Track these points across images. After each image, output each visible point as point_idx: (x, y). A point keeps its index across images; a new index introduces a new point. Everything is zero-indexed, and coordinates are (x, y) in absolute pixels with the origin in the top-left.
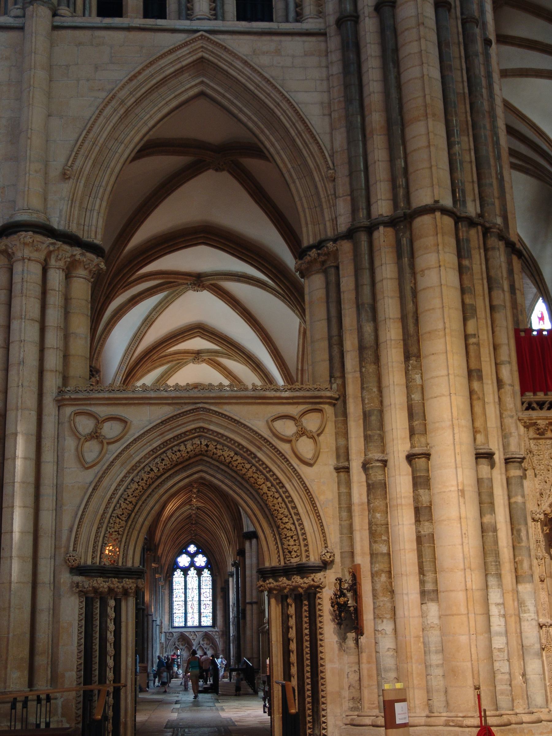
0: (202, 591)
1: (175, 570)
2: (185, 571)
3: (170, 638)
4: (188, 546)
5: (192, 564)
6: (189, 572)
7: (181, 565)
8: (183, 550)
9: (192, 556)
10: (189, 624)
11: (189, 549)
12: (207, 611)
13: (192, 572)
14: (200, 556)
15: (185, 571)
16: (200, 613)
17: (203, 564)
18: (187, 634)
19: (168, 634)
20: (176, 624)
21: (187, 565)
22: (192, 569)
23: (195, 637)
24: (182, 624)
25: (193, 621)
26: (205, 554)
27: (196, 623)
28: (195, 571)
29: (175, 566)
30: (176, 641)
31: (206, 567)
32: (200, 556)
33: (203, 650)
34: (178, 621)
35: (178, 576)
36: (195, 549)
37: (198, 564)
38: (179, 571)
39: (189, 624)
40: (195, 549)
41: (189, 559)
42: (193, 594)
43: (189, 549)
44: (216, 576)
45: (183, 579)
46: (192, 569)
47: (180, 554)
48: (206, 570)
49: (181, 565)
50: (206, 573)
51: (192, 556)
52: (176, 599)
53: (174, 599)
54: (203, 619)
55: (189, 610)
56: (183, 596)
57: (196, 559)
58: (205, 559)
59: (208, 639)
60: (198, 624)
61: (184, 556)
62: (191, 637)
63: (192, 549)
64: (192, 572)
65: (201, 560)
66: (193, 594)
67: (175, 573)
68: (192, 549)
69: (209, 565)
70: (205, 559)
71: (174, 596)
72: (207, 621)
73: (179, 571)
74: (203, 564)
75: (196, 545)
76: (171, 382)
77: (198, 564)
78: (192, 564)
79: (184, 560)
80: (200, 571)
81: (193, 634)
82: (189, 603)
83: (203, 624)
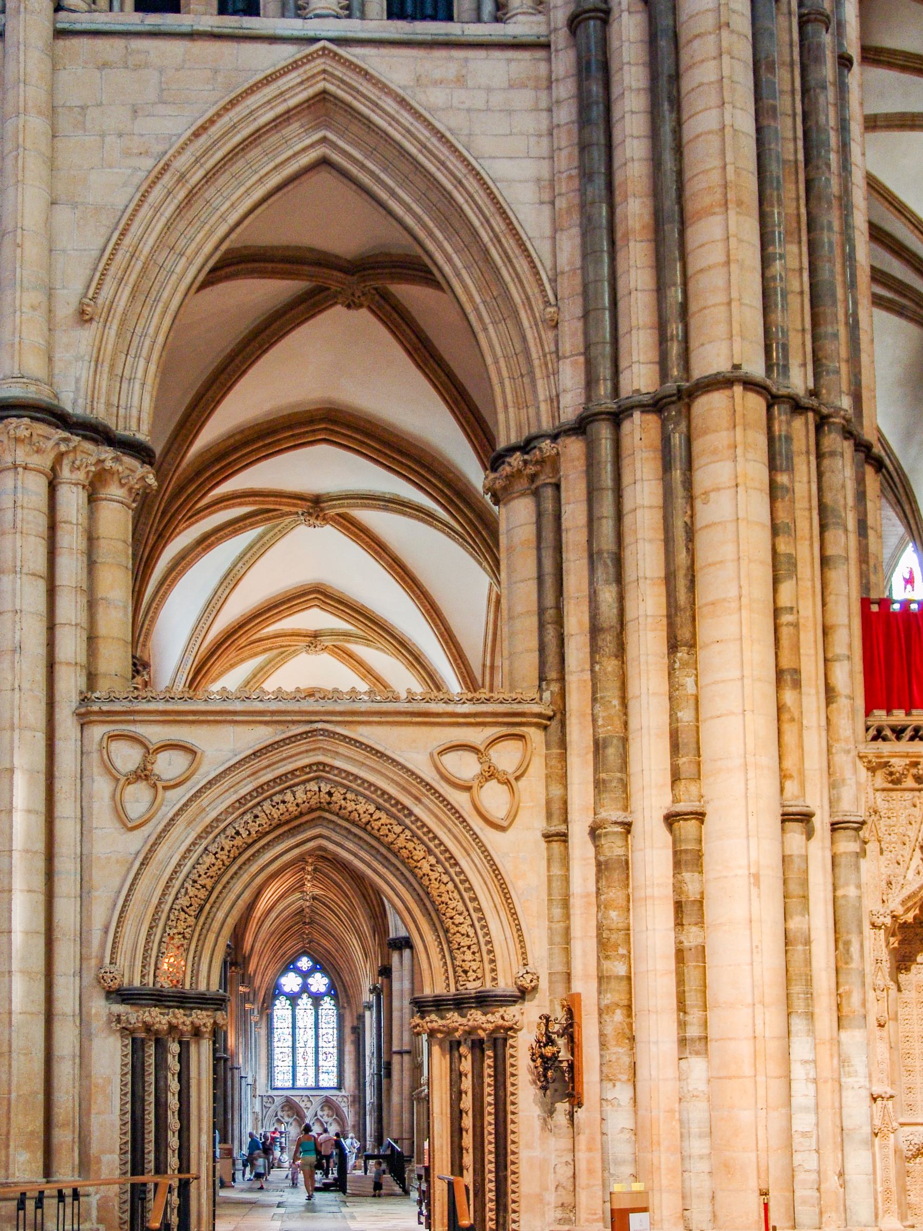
0: (321, 1032)
1: (275, 997)
2: (293, 998)
4: (297, 958)
5: (305, 988)
6: (300, 1001)
8: (289, 966)
9: (305, 975)
10: (300, 1083)
11: (299, 964)
12: (329, 1063)
13: (305, 1002)
14: (318, 975)
15: (293, 998)
16: (317, 1066)
17: (323, 989)
18: (296, 1099)
19: (265, 1099)
20: (278, 1084)
22: (305, 996)
23: (309, 1105)
25: (306, 1078)
26: (325, 972)
27: (311, 1083)
29: (275, 992)
30: (279, 1109)
31: (327, 993)
33: (322, 1124)
34: (282, 1079)
35: (281, 1008)
36: (310, 964)
37: (313, 989)
38: (282, 998)
39: (300, 1083)
40: (310, 964)
41: (299, 980)
42: (306, 1037)
43: (299, 964)
44: (344, 1008)
45: (290, 1012)
46: (305, 996)
47: (285, 970)
48: (327, 999)
49: (287, 989)
50: (328, 1004)
51: (305, 975)
52: (280, 1044)
53: (276, 1044)
54: (321, 1076)
55: (300, 1062)
56: (290, 1038)
57: (310, 981)
58: (326, 980)
59: (330, 1108)
61: (292, 975)
62: (302, 1105)
64: (305, 1002)
65: (319, 982)
66: (306, 1037)
67: (277, 1002)
68: (305, 963)
69: (333, 991)
70: (326, 980)
71: (276, 1039)
72: (329, 1080)
73: (282, 998)
74: (323, 989)
75: (312, 958)
76: (270, 685)
77: (313, 989)
78: (305, 988)
79: (290, 982)
80: (317, 999)
81: (305, 1099)
82: (300, 1051)
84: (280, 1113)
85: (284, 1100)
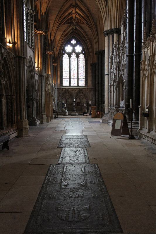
0: (79, 66)
2: (69, 55)
5: (74, 51)
6: (72, 55)
7: (67, 51)
9: (74, 46)
10: (72, 85)
12: (82, 76)
13: (74, 56)
14: (78, 46)
15: (69, 55)
21: (71, 51)
22: (74, 53)
24: (68, 85)
25: (74, 83)
26: (81, 45)
27: (76, 84)
28: (75, 55)
29: (62, 52)
31: (82, 53)
32: (78, 46)
34: (66, 83)
37: (77, 51)
38: (66, 54)
39: (72, 85)
40: (75, 42)
43: (72, 42)
45: (68, 59)
46: (74, 53)
47: (66, 44)
48: (81, 54)
50: (82, 56)
51: (74, 46)
55: (72, 77)
60: (77, 85)
62: (73, 92)
63: (74, 42)
64: (74, 56)
65: (79, 49)
66: (74, 68)
67: (64, 56)
68: (74, 42)
69: (84, 52)
71: (63, 69)
72: (82, 83)
73: (66, 54)
78: (74, 51)
79: (69, 49)
80: (78, 55)
83: (80, 85)
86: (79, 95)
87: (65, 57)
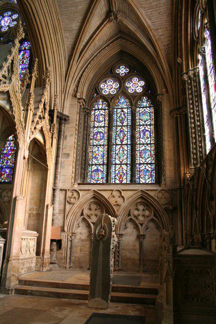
3: (73, 200)
5: (122, 91)
9: (121, 80)
14: (135, 79)
18: (106, 195)
19: (69, 194)
23: (120, 201)
41: (116, 85)
42: (122, 136)
62: (112, 201)
64: (123, 102)
65: (136, 85)
66: (122, 136)
69: (150, 91)
78: (122, 91)
80: (134, 100)
81: (119, 195)
84: (86, 212)
85: (90, 195)
86: (136, 213)
87: (101, 104)
